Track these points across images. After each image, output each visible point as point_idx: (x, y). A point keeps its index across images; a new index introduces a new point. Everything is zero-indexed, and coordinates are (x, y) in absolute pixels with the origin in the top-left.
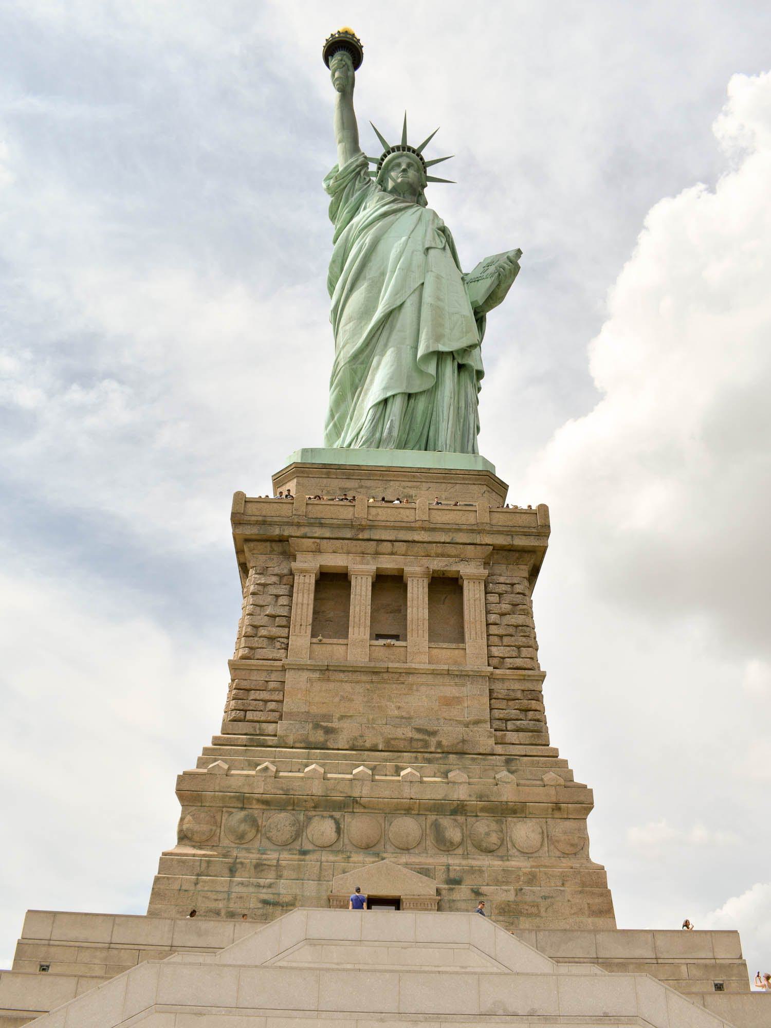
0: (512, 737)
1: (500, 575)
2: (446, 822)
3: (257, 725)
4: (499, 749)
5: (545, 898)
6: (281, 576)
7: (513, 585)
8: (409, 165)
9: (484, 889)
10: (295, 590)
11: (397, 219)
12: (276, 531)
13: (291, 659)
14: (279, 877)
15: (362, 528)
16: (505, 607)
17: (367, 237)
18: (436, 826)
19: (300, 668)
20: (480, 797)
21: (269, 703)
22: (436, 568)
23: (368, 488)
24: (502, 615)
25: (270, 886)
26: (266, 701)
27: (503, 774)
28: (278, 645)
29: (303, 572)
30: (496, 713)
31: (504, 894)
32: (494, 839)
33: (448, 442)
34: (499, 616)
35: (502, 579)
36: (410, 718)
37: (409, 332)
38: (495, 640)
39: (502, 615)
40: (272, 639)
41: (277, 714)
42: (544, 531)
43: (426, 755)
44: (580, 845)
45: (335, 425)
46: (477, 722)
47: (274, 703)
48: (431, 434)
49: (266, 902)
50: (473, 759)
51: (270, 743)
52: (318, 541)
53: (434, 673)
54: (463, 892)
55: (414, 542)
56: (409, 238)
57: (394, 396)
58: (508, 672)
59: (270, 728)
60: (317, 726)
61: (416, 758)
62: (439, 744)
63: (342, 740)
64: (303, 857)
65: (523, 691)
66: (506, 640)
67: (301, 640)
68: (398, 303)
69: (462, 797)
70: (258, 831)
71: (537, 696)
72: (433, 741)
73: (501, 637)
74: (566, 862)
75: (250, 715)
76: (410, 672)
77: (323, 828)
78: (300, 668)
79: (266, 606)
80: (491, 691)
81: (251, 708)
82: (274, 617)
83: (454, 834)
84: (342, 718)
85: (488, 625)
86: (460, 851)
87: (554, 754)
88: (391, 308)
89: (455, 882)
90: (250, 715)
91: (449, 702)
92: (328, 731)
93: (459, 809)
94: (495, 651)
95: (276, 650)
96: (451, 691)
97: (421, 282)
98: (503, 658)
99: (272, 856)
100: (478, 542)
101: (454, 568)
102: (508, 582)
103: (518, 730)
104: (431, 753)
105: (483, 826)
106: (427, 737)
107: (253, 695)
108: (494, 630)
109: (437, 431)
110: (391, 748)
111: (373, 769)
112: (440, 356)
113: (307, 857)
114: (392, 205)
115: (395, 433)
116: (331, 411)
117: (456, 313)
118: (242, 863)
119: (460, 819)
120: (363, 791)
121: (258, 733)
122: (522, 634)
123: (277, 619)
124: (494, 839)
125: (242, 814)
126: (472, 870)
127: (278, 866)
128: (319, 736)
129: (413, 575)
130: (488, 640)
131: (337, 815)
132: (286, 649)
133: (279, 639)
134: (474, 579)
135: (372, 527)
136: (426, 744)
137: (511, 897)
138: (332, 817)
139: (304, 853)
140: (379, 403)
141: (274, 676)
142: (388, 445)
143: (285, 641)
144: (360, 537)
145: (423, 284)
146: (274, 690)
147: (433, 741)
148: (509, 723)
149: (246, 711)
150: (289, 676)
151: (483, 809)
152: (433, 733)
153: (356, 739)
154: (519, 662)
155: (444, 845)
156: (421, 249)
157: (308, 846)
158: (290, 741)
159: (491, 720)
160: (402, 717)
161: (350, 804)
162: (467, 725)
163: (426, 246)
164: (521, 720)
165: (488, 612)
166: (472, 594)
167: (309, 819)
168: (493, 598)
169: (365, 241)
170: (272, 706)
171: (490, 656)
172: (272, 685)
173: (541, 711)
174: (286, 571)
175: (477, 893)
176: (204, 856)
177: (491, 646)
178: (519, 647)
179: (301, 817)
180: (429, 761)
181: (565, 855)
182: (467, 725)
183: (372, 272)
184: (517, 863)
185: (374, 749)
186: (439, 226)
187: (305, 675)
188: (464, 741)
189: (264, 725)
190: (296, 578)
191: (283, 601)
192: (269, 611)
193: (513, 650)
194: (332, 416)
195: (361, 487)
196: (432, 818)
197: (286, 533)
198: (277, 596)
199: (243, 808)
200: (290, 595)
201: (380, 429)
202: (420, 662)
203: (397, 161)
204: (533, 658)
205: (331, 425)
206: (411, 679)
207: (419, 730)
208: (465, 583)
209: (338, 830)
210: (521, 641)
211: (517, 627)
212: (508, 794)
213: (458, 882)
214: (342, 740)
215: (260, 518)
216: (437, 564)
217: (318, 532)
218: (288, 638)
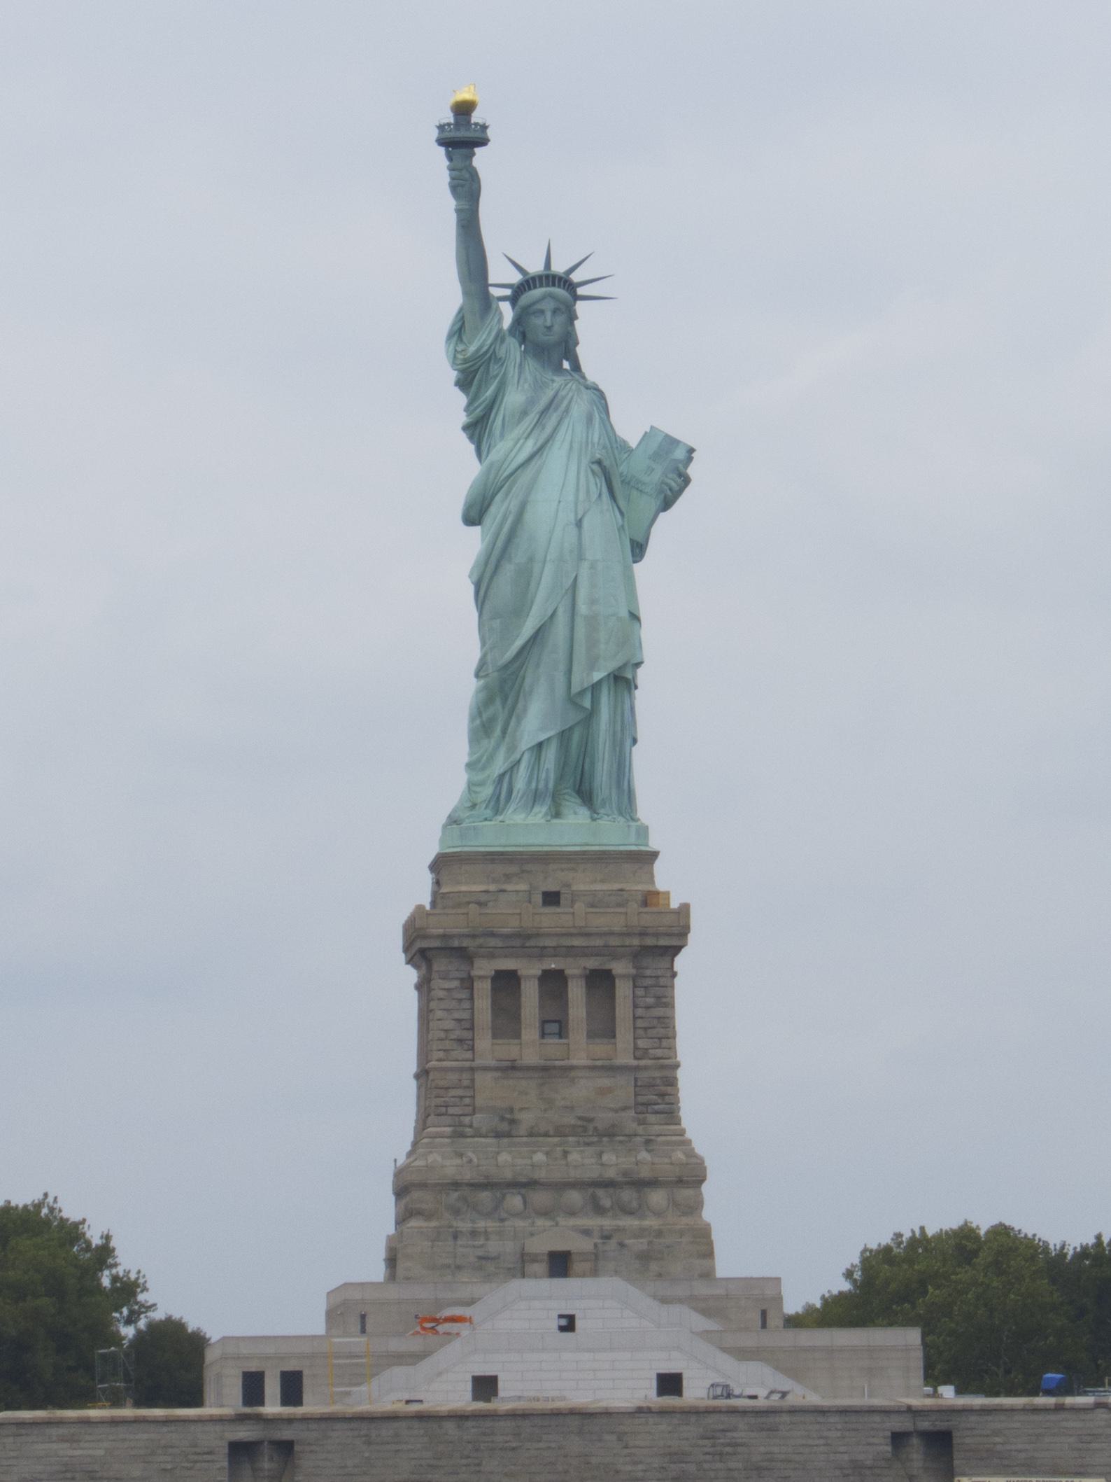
0: (652, 1118)
1: (647, 968)
2: (600, 1193)
3: (457, 1118)
4: (640, 1130)
5: (668, 1247)
6: (462, 980)
7: (657, 977)
8: (555, 312)
9: (627, 1242)
10: (475, 996)
11: (545, 461)
12: (456, 943)
13: (478, 1062)
14: (487, 1239)
15: (529, 937)
16: (650, 1000)
17: (510, 501)
18: (594, 1198)
19: (486, 1069)
20: (625, 1174)
21: (465, 1099)
22: (592, 967)
23: (528, 872)
24: (648, 1008)
25: (482, 1246)
26: (461, 1097)
27: (644, 1155)
28: (466, 1047)
29: (481, 978)
30: (640, 1099)
31: (640, 1245)
32: (635, 1204)
33: (603, 787)
34: (644, 1009)
35: (648, 972)
36: (572, 1108)
37: (561, 655)
38: (640, 1032)
39: (648, 1008)
40: (460, 1041)
41: (471, 1108)
42: (683, 932)
43: (586, 1140)
44: (695, 1207)
45: (483, 725)
46: (625, 1109)
47: (468, 1099)
48: (586, 767)
49: (480, 1258)
50: (621, 1142)
51: (469, 1134)
52: (491, 950)
53: (593, 1068)
54: (613, 1243)
55: (573, 947)
56: (560, 502)
57: (548, 739)
58: (649, 1062)
59: (467, 1120)
60: (502, 1119)
61: (579, 1142)
62: (596, 1129)
63: (523, 1129)
64: (501, 1225)
65: (662, 1078)
66: (651, 1033)
67: (484, 1042)
68: (549, 613)
69: (612, 1176)
70: (468, 1206)
71: (672, 1082)
72: (591, 1127)
73: (646, 1029)
74: (685, 1220)
75: (451, 1110)
76: (572, 1068)
77: (515, 1201)
78: (486, 1069)
79: (452, 1009)
80: (636, 1080)
81: (451, 1104)
82: (459, 1021)
83: (606, 1202)
84: (521, 1109)
85: (635, 1018)
86: (610, 1214)
87: (682, 1133)
88: (543, 622)
89: (607, 1237)
90: (451, 1110)
91: (603, 1092)
92: (513, 1122)
93: (609, 1184)
94: (641, 1043)
95: (465, 1052)
96: (605, 1082)
97: (574, 575)
98: (647, 1049)
99: (481, 1224)
100: (627, 944)
101: (607, 967)
102: (653, 975)
103: (657, 1112)
104: (590, 1136)
105: (627, 1195)
106: (585, 1123)
107: (453, 1092)
108: (640, 1023)
109: (593, 764)
110: (560, 1132)
111: (547, 1154)
112: (596, 687)
113: (507, 1223)
114: (536, 432)
115: (551, 785)
116: (479, 708)
117: (612, 616)
118: (461, 1232)
119: (611, 1190)
120: (541, 1175)
121: (457, 1124)
122: (663, 1026)
123: (463, 1023)
124: (635, 1204)
125: (456, 1195)
126: (619, 1230)
127: (486, 1231)
128: (504, 1127)
129: (574, 976)
130: (634, 1032)
131: (523, 1191)
132: (472, 1049)
133: (466, 1042)
134: (623, 976)
135: (538, 935)
136: (585, 1129)
137: (645, 1247)
138: (519, 1193)
139: (502, 1220)
140: (531, 749)
141: (466, 1076)
142: (544, 800)
143: (471, 1042)
144: (527, 945)
145: (576, 577)
146: (468, 1087)
147: (591, 1127)
148: (649, 1107)
149: (447, 1106)
150: (479, 1077)
151: (627, 1183)
152: (590, 1120)
153: (532, 1128)
154: (659, 1052)
155: (599, 1210)
156: (572, 517)
157: (504, 1215)
158: (484, 1130)
159: (637, 1104)
160: (566, 1107)
161: (532, 1184)
162: (616, 1111)
163: (579, 517)
164: (658, 1104)
165: (635, 1006)
166: (623, 990)
167: (504, 1196)
168: (640, 992)
169: (509, 504)
170: (467, 1101)
171: (636, 1048)
172: (466, 1083)
173: (675, 1095)
174: (464, 975)
175: (622, 1245)
176: (435, 1227)
177: (637, 1038)
178: (660, 1039)
179: (498, 1195)
180: (588, 1144)
181: (685, 1214)
182: (616, 1111)
183: (519, 556)
184: (651, 1222)
185: (546, 1135)
186: (594, 460)
187: (489, 1076)
188: (613, 1126)
189: (462, 1118)
190: (475, 984)
191: (466, 1005)
192: (457, 1015)
193: (655, 1042)
194: (480, 713)
195: (523, 872)
196: (591, 1190)
197: (464, 945)
198: (460, 1000)
199: (456, 1190)
200: (472, 999)
201: (535, 776)
202: (580, 1059)
203: (538, 306)
204: (672, 1048)
205: (478, 722)
206: (573, 1074)
207: (580, 1118)
208: (617, 981)
209: (525, 1202)
210: (662, 1032)
211: (659, 1018)
212: (645, 1173)
213: (608, 1237)
214: (523, 1129)
215: (441, 931)
216: (592, 963)
217: (493, 942)
218: (473, 1040)
